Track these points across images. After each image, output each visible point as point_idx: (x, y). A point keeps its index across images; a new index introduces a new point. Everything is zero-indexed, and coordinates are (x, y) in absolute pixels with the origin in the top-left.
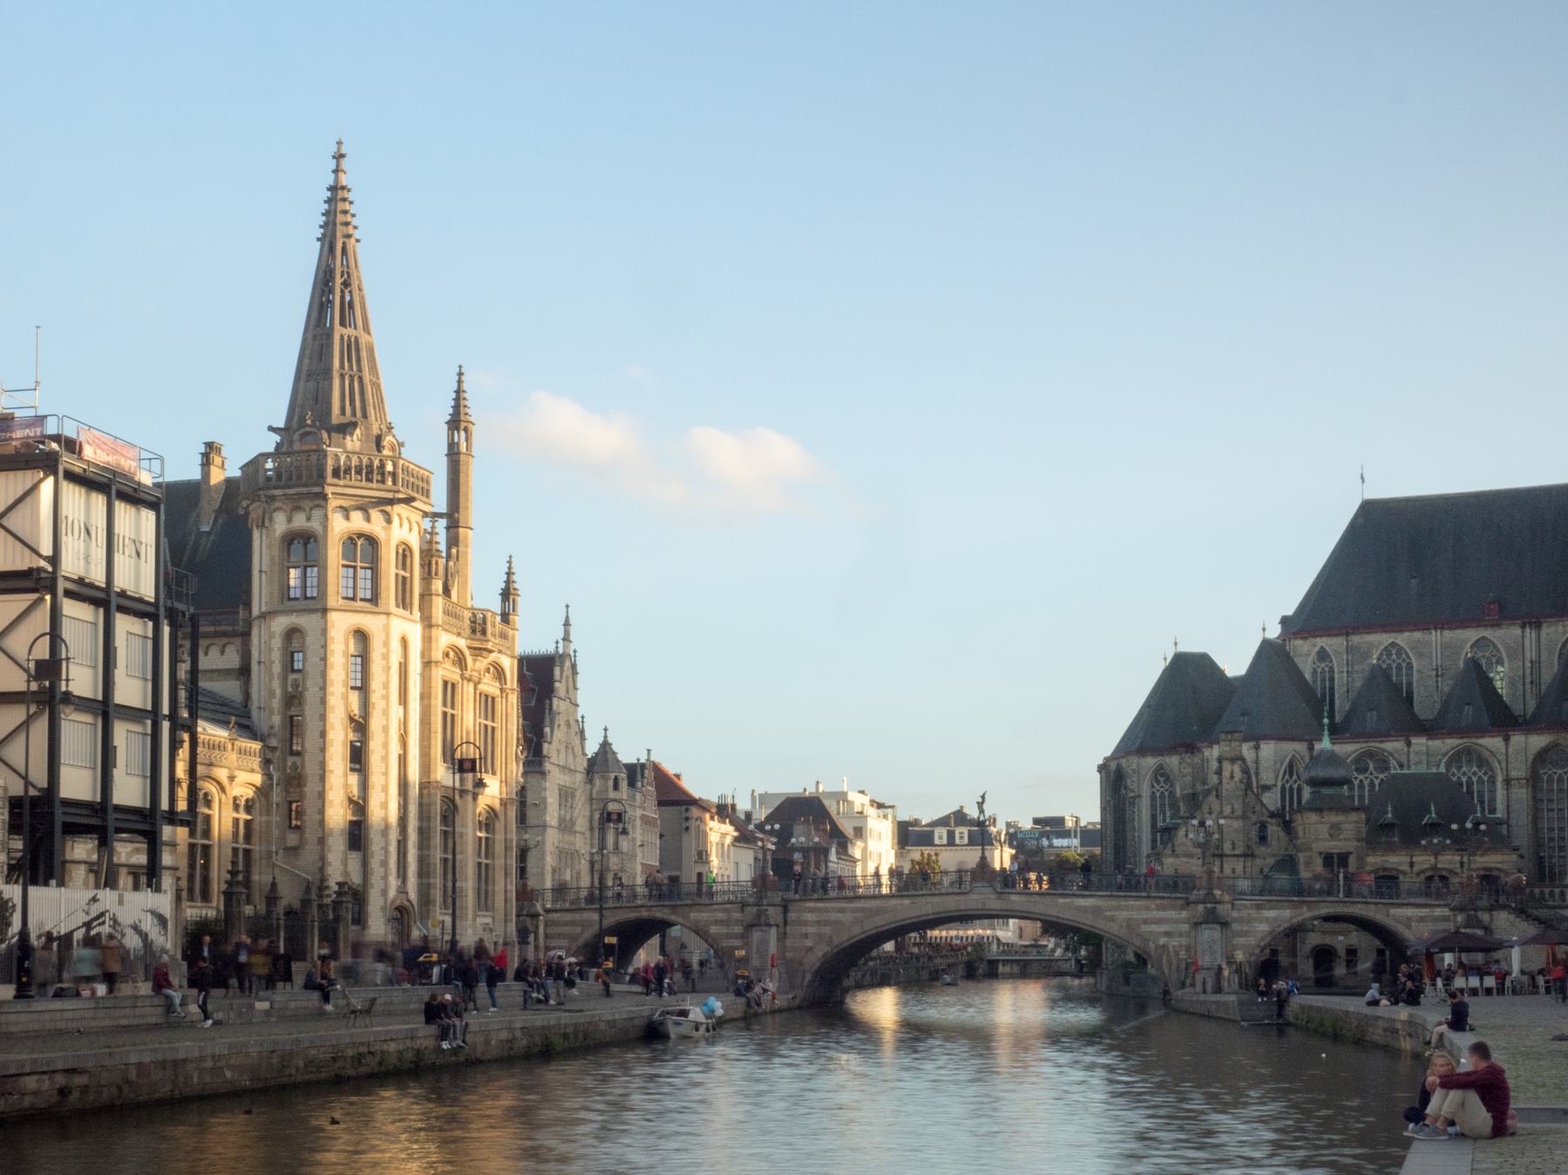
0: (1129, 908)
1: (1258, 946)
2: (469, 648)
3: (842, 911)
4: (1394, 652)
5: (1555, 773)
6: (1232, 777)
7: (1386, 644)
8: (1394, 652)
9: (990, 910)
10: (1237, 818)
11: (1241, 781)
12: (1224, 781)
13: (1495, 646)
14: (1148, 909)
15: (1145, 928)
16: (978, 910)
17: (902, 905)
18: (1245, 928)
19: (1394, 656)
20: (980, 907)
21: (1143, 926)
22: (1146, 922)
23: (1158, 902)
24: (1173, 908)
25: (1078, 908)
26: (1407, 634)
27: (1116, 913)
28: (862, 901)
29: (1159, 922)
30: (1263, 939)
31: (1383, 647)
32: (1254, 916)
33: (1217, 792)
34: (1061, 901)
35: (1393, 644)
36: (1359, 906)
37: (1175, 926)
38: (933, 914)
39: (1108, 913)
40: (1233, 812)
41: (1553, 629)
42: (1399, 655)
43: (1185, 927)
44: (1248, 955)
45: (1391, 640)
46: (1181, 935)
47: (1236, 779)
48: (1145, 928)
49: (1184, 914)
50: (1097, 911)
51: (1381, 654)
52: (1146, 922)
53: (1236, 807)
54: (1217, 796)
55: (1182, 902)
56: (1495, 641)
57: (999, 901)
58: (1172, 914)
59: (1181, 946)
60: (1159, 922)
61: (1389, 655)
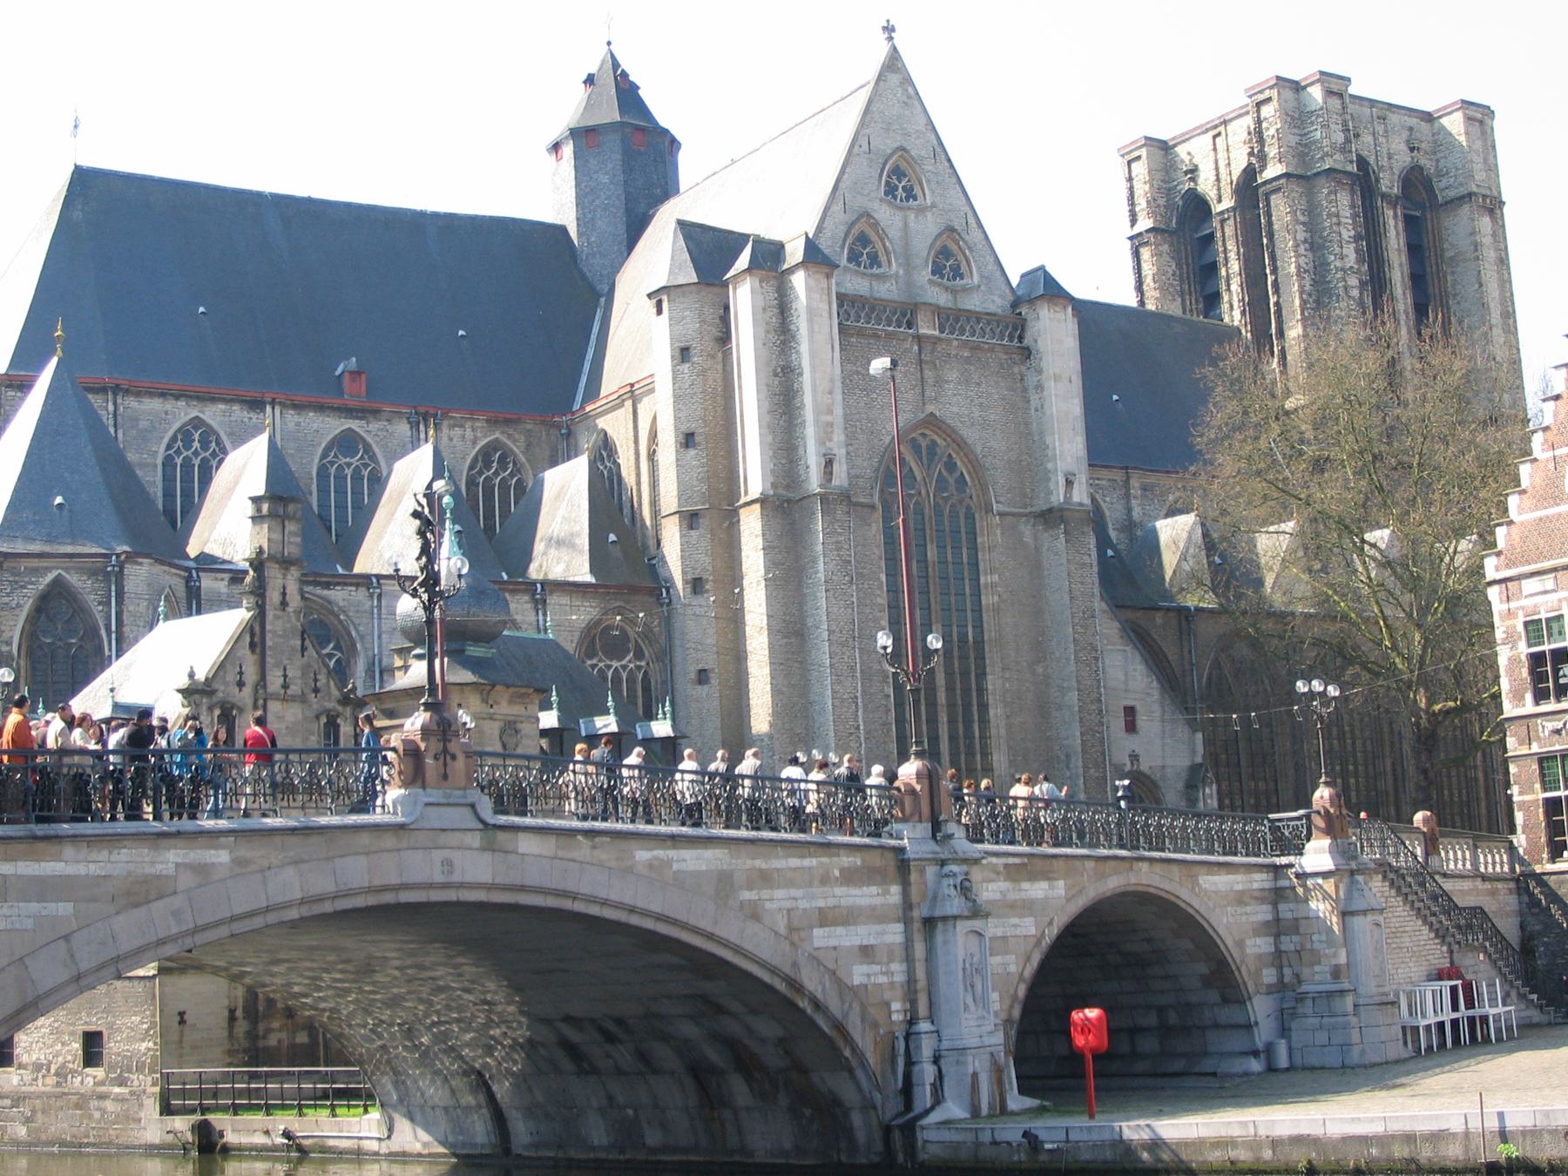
4: (197, 436)
5: (610, 666)
6: (284, 604)
7: (185, 419)
8: (197, 436)
9: (462, 886)
10: (293, 699)
11: (297, 612)
12: (270, 615)
13: (368, 448)
15: (822, 937)
16: (431, 886)
17: (202, 870)
19: (196, 444)
20: (439, 878)
21: (817, 932)
22: (826, 918)
23: (846, 860)
25: (680, 880)
26: (222, 406)
27: (765, 894)
28: (69, 851)
29: (847, 917)
30: (1028, 959)
31: (176, 426)
33: (252, 635)
34: (643, 855)
35: (197, 423)
36: (1158, 868)
38: (302, 902)
39: (747, 895)
40: (285, 686)
41: (458, 431)
42: (205, 444)
43: (894, 934)
44: (1005, 1007)
45: (194, 413)
47: (290, 609)
48: (822, 937)
50: (724, 882)
51: (174, 439)
52: (826, 918)
53: (290, 674)
54: (252, 646)
56: (369, 439)
57: (488, 856)
58: (866, 896)
60: (847, 917)
61: (188, 443)
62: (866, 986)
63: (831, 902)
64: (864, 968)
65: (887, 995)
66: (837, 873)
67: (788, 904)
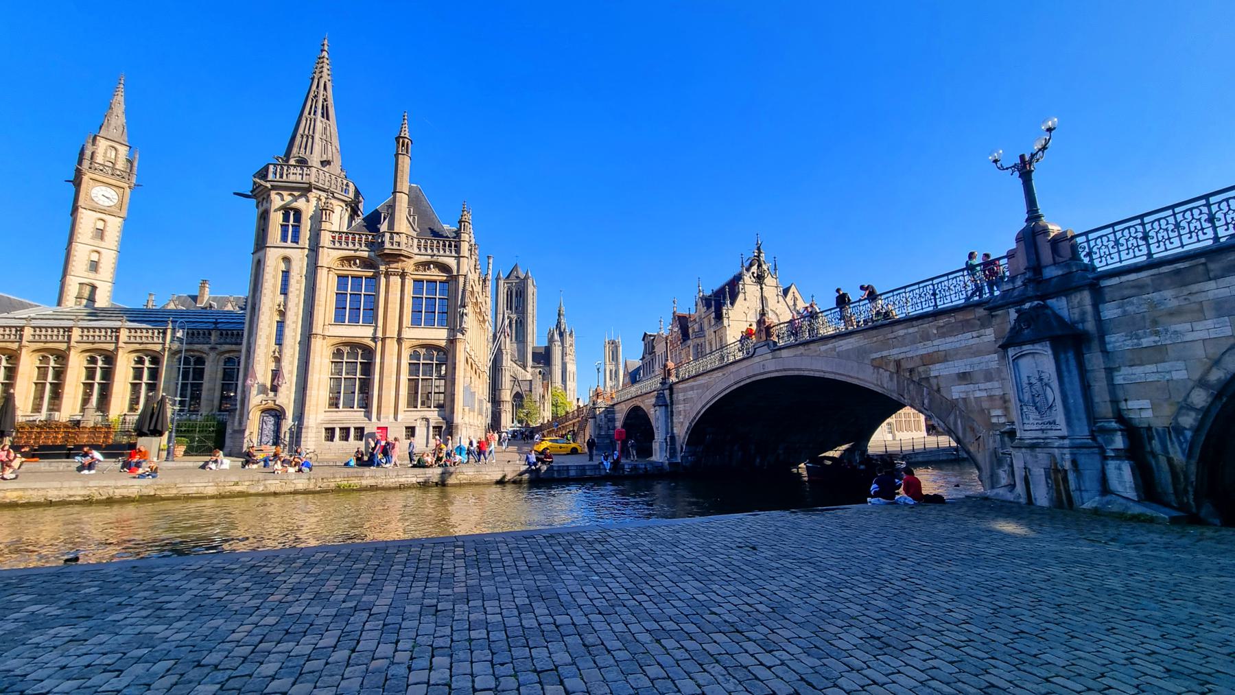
0: (902, 341)
1: (1202, 383)
2: (379, 256)
3: (692, 388)
14: (926, 337)
18: (1145, 342)
24: (966, 326)
32: (1174, 303)
37: (976, 360)
38: (736, 384)
39: (875, 356)
43: (992, 361)
44: (1167, 410)
46: (988, 377)
49: (989, 335)
55: (981, 312)
59: (991, 397)
62: (964, 399)
63: (930, 350)
64: (963, 388)
65: (985, 405)
66: (935, 332)
67: (901, 356)
